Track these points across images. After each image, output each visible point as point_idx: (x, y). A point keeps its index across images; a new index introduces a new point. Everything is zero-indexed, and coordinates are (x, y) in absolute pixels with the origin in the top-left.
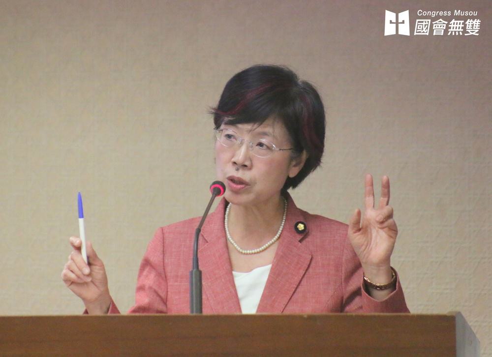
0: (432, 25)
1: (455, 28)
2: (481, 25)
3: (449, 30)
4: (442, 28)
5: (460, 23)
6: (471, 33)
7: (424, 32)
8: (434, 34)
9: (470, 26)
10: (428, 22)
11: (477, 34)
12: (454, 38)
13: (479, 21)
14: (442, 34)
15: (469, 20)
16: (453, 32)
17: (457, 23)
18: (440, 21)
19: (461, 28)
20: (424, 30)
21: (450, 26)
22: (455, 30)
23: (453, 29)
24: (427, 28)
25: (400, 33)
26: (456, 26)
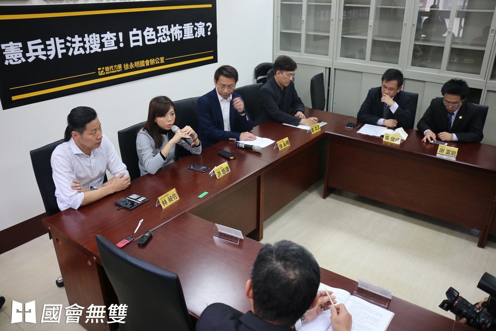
1: (94, 314)
2: (128, 311)
3: (87, 317)
4: (77, 314)
6: (116, 321)
8: (67, 322)
9: (114, 312)
11: (124, 322)
13: (125, 306)
15: (112, 305)
16: (92, 320)
17: (97, 309)
18: (75, 307)
19: (102, 314)
20: (54, 317)
21: (87, 312)
22: (94, 317)
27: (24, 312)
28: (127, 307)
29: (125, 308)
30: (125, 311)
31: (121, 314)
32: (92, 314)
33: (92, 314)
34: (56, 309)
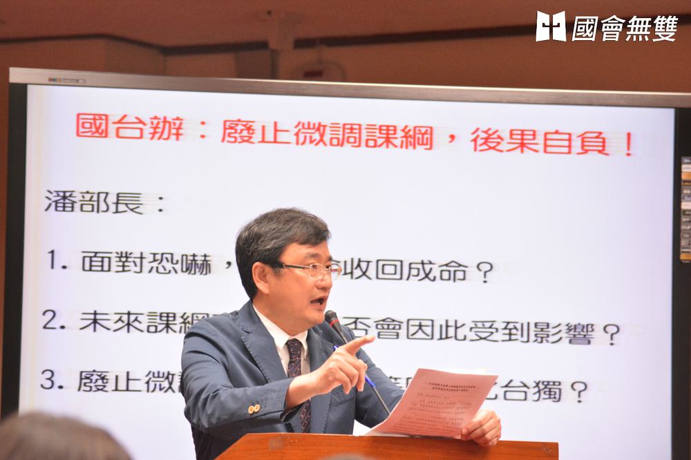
0: (600, 25)
1: (637, 29)
3: (628, 33)
4: (616, 29)
5: (645, 22)
6: (663, 38)
7: (587, 36)
8: (604, 39)
9: (661, 27)
10: (594, 20)
11: (673, 40)
12: (638, 45)
13: (675, 18)
14: (617, 40)
15: (659, 17)
16: (635, 37)
17: (640, 22)
18: (614, 19)
19: (646, 29)
20: (588, 33)
21: (628, 26)
22: (636, 32)
23: (634, 30)
24: (593, 30)
25: (555, 38)
26: (639, 27)
27: (551, 26)
28: (677, 19)
29: (675, 21)
30: (675, 25)
31: (670, 28)
32: (635, 28)
33: (635, 28)
34: (590, 23)
